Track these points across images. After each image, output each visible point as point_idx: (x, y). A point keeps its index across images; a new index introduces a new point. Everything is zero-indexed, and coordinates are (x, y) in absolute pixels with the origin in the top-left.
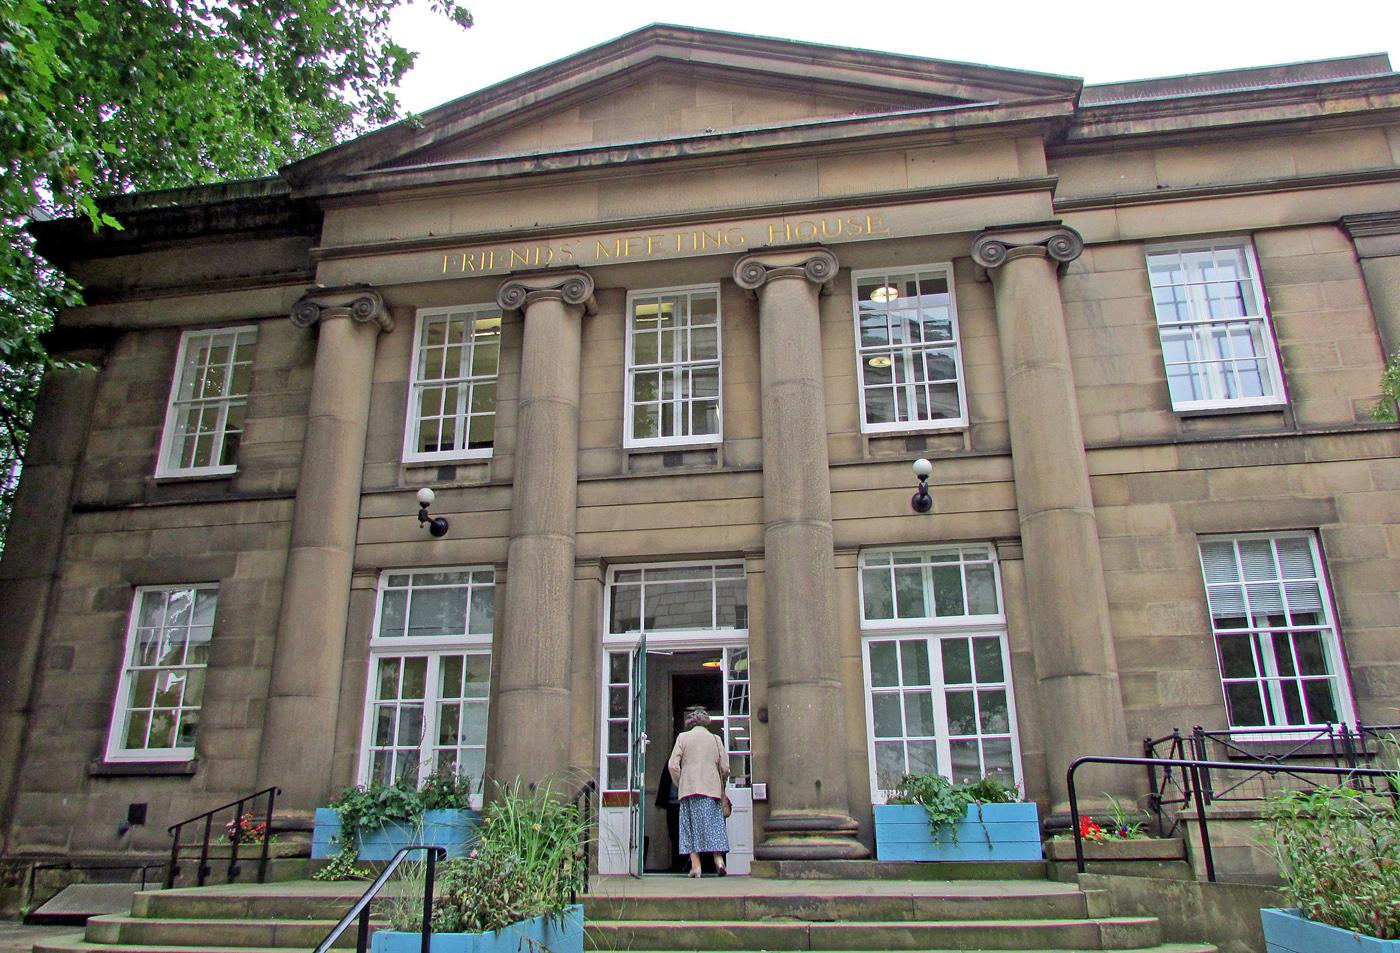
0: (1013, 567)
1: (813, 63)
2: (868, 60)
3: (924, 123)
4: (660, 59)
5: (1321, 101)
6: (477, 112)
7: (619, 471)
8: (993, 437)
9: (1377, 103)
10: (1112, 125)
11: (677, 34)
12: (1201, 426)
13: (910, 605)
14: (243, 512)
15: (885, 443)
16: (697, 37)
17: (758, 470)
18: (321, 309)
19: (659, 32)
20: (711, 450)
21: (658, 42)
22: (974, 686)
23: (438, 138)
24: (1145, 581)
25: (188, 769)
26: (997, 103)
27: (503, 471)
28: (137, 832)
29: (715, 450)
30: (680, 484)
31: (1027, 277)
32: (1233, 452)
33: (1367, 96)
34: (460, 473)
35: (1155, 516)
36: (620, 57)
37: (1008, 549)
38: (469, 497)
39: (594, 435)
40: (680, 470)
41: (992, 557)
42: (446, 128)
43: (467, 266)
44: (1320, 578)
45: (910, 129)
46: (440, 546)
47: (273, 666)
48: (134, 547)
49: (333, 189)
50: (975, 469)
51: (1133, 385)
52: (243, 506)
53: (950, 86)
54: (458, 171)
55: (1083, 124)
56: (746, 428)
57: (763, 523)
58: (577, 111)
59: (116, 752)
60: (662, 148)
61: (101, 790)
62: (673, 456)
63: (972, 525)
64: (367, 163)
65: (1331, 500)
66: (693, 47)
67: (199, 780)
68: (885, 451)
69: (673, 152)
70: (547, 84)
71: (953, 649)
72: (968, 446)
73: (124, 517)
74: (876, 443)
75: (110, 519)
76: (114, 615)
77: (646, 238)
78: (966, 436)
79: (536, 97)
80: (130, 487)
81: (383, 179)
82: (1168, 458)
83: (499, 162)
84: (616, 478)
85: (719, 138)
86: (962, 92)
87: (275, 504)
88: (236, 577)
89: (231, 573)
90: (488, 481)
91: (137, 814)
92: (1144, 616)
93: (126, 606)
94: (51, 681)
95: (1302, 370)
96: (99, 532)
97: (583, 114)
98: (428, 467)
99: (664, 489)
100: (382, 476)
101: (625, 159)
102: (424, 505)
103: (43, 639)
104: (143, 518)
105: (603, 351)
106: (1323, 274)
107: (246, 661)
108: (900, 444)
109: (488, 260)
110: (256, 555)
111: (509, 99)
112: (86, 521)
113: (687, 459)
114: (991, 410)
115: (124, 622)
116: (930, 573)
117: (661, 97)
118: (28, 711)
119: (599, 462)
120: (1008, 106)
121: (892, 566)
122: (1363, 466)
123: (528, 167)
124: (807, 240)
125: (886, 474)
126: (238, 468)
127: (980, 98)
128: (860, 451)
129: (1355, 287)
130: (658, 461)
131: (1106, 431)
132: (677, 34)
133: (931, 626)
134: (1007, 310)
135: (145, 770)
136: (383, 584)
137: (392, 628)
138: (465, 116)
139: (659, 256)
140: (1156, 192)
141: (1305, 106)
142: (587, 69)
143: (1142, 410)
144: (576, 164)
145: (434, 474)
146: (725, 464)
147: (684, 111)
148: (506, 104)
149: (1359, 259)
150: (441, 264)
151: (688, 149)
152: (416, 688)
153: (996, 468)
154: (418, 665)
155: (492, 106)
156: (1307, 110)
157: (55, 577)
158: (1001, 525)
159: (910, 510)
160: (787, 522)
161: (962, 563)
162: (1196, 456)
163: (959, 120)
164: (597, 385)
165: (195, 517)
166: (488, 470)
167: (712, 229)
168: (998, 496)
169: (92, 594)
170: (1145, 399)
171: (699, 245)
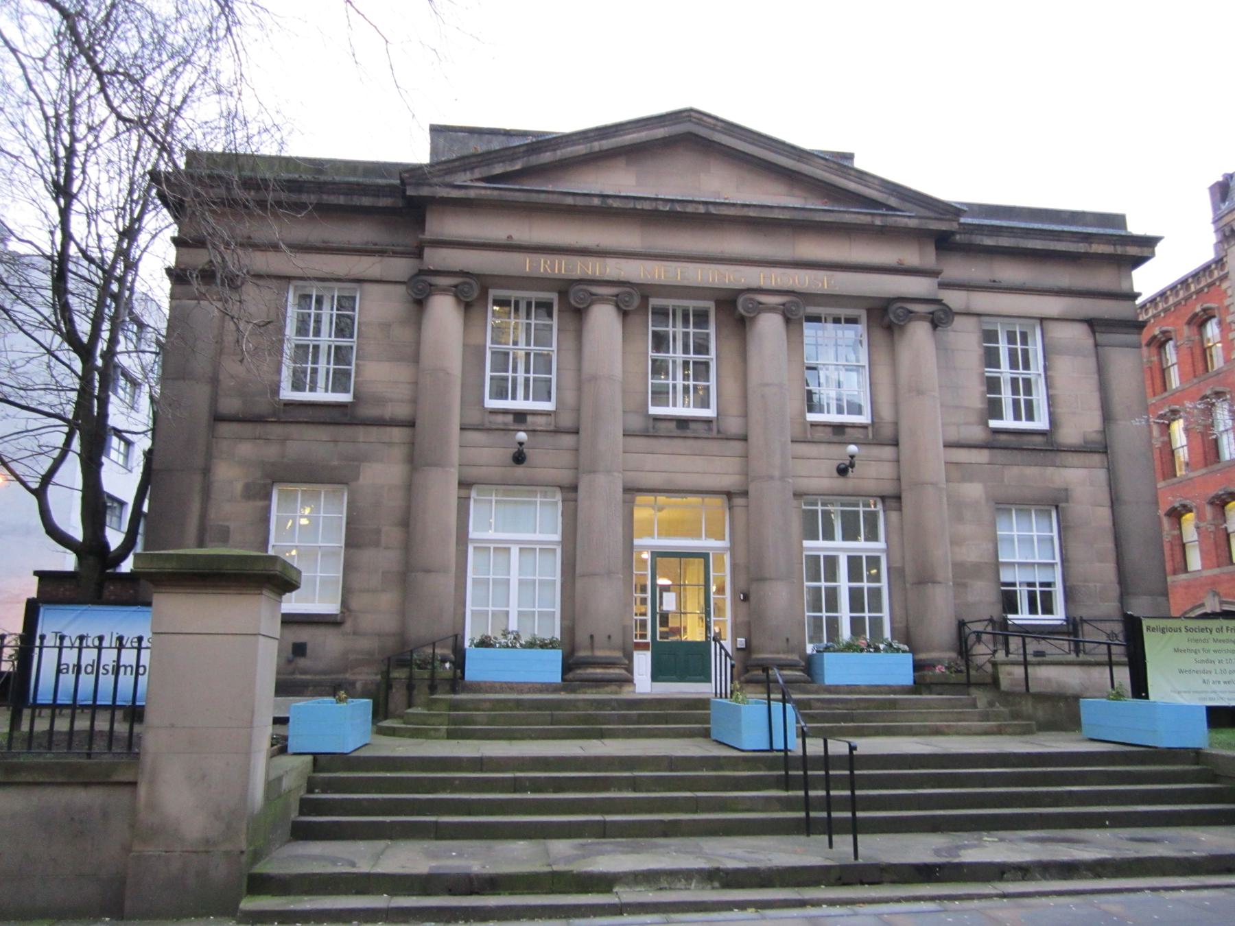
0: (894, 515)
1: (798, 161)
3: (868, 219)
4: (690, 134)
5: (1091, 243)
6: (555, 150)
7: (647, 430)
8: (887, 432)
9: (1119, 250)
10: (973, 237)
11: (705, 118)
12: (1003, 437)
13: (829, 535)
14: (361, 433)
15: (819, 428)
16: (720, 124)
17: (744, 439)
18: (431, 285)
19: (693, 114)
20: (708, 421)
21: (690, 121)
22: (823, 584)
24: (967, 529)
25: (339, 619)
26: (913, 214)
27: (566, 420)
28: (302, 662)
30: (690, 442)
31: (919, 333)
32: (1018, 456)
33: (1114, 245)
34: (529, 418)
35: (974, 491)
36: (663, 127)
37: (893, 503)
38: (541, 439)
40: (689, 433)
41: (880, 507)
43: (545, 269)
44: (1055, 534)
46: (520, 471)
47: (407, 546)
48: (271, 452)
50: (876, 451)
53: (885, 196)
54: (543, 196)
56: (734, 408)
57: (745, 473)
62: (683, 423)
63: (871, 486)
65: (1066, 490)
66: (717, 131)
67: (348, 626)
68: (820, 434)
69: (702, 209)
70: (607, 138)
71: (854, 562)
72: (870, 436)
73: (259, 429)
74: (813, 428)
75: (247, 429)
76: (261, 503)
77: (676, 268)
78: (870, 429)
79: (600, 145)
80: (262, 406)
81: (483, 192)
82: (982, 456)
83: (574, 194)
84: (645, 434)
85: (734, 205)
86: (893, 202)
87: (388, 429)
89: (356, 478)
90: (552, 428)
93: (268, 497)
95: (1061, 410)
96: (240, 439)
98: (505, 412)
100: (474, 417)
101: (667, 209)
102: (521, 444)
103: (203, 516)
104: (277, 430)
107: (376, 544)
109: (561, 267)
111: (579, 144)
112: (225, 429)
113: (692, 425)
114: (886, 414)
115: (268, 509)
116: (839, 513)
119: (636, 423)
120: (920, 218)
121: (820, 508)
123: (596, 202)
124: (786, 287)
125: (823, 449)
127: (903, 209)
128: (805, 432)
129: (1091, 363)
131: (953, 436)
132: (705, 118)
133: (841, 548)
134: (905, 356)
138: (546, 151)
139: (685, 283)
141: (1081, 245)
142: (639, 132)
145: (510, 418)
146: (719, 432)
149: (1096, 345)
150: (526, 264)
151: (713, 210)
153: (888, 452)
156: (1081, 247)
157: (206, 471)
158: (888, 488)
159: (835, 474)
160: (771, 478)
161: (861, 509)
162: (1000, 455)
163: (891, 221)
165: (322, 433)
167: (723, 268)
168: (887, 470)
169: (239, 487)
171: (714, 280)
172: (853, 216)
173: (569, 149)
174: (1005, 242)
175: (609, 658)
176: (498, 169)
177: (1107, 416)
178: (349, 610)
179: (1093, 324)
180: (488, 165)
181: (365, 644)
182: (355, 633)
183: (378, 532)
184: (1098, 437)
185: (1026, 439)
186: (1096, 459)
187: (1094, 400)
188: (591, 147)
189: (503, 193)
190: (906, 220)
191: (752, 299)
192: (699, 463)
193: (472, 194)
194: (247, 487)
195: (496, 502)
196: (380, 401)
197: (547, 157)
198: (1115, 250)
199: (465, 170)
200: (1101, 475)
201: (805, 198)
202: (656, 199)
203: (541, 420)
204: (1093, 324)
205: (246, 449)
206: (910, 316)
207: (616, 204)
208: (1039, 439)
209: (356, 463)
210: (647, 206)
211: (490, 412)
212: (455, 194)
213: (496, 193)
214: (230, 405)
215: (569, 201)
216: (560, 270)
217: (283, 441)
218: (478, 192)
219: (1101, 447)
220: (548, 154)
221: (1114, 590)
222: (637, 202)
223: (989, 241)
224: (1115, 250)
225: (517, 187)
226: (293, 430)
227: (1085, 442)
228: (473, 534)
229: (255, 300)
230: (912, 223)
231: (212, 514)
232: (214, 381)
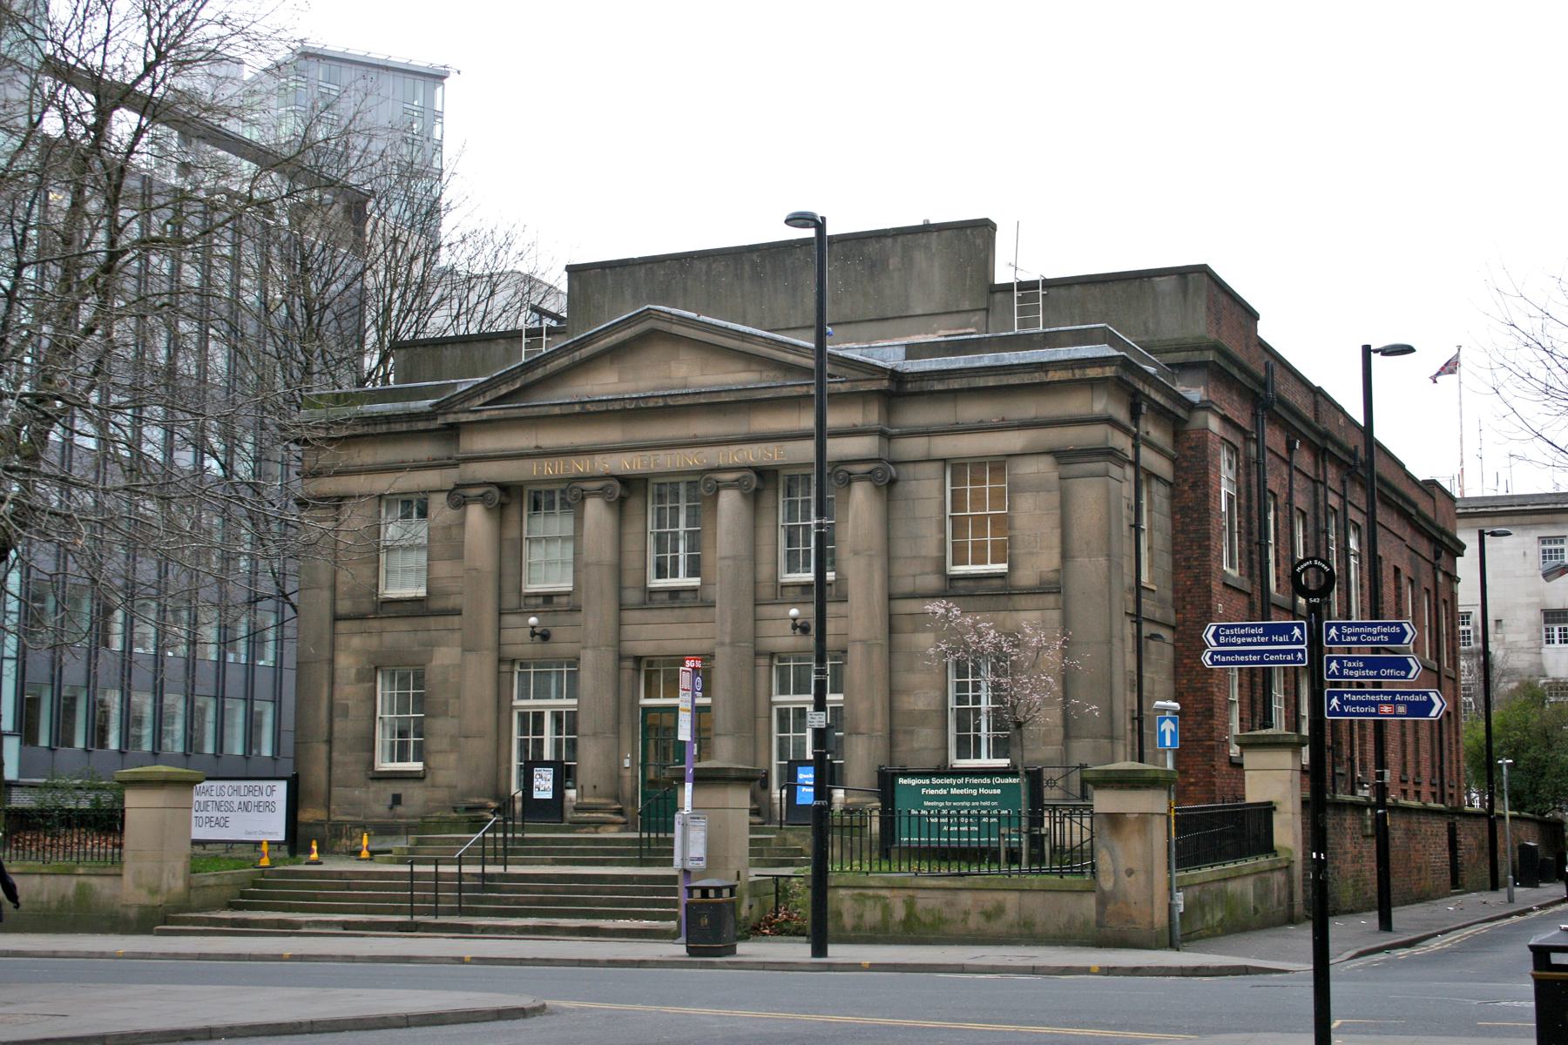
5: (1047, 371)
9: (1078, 374)
11: (662, 314)
14: (432, 622)
15: (791, 589)
25: (421, 775)
28: (399, 809)
29: (696, 590)
30: (677, 612)
34: (555, 600)
36: (629, 328)
38: (562, 618)
39: (629, 580)
45: (795, 394)
48: (373, 642)
49: (464, 418)
51: (925, 557)
52: (432, 619)
54: (536, 409)
55: (908, 382)
58: (609, 356)
59: (384, 765)
60: (655, 400)
61: (376, 786)
62: (674, 593)
64: (482, 401)
67: (428, 780)
68: (790, 593)
69: (661, 403)
70: (585, 347)
76: (371, 684)
78: (834, 586)
81: (493, 412)
88: (434, 663)
89: (431, 661)
91: (397, 799)
92: (912, 700)
93: (376, 682)
94: (338, 725)
96: (353, 634)
97: (612, 361)
99: (666, 615)
101: (633, 406)
104: (375, 624)
105: (633, 529)
106: (1038, 488)
107: (445, 714)
108: (798, 589)
110: (444, 649)
112: (342, 626)
113: (683, 595)
117: (658, 351)
118: (330, 742)
120: (851, 381)
122: (1038, 614)
123: (577, 408)
126: (427, 593)
129: (1055, 498)
130: (665, 596)
132: (662, 314)
135: (393, 775)
136: (517, 668)
137: (524, 695)
138: (537, 368)
141: (1036, 374)
143: (928, 574)
144: (604, 408)
145: (540, 600)
146: (702, 600)
147: (673, 363)
148: (562, 360)
151: (670, 402)
152: (539, 730)
154: (539, 717)
156: (1037, 377)
157: (332, 661)
164: (632, 545)
166: (571, 598)
169: (353, 672)
170: (929, 567)
172: (790, 389)
173: (556, 362)
175: (592, 804)
176: (504, 390)
177: (1065, 555)
178: (430, 768)
179: (1062, 456)
180: (495, 388)
181: (441, 794)
182: (433, 786)
183: (446, 703)
184: (1052, 576)
185: (985, 583)
186: (1050, 600)
187: (1055, 539)
189: (507, 411)
190: (839, 385)
191: (710, 479)
192: (683, 631)
193: (485, 415)
194: (359, 672)
196: (447, 594)
197: (539, 373)
198: (1074, 375)
200: (1055, 615)
201: (761, 371)
203: (564, 600)
204: (1062, 456)
205: (356, 642)
206: (848, 481)
208: (996, 583)
209: (429, 648)
210: (617, 406)
212: (472, 417)
213: (502, 412)
214: (344, 606)
215: (557, 410)
216: (559, 471)
217: (381, 633)
218: (488, 413)
219: (1052, 588)
220: (540, 370)
221: (1058, 735)
222: (609, 404)
223: (939, 386)
224: (1074, 375)
226: (386, 624)
227: (1041, 583)
229: (355, 519)
230: (843, 388)
231: (337, 695)
232: (334, 588)
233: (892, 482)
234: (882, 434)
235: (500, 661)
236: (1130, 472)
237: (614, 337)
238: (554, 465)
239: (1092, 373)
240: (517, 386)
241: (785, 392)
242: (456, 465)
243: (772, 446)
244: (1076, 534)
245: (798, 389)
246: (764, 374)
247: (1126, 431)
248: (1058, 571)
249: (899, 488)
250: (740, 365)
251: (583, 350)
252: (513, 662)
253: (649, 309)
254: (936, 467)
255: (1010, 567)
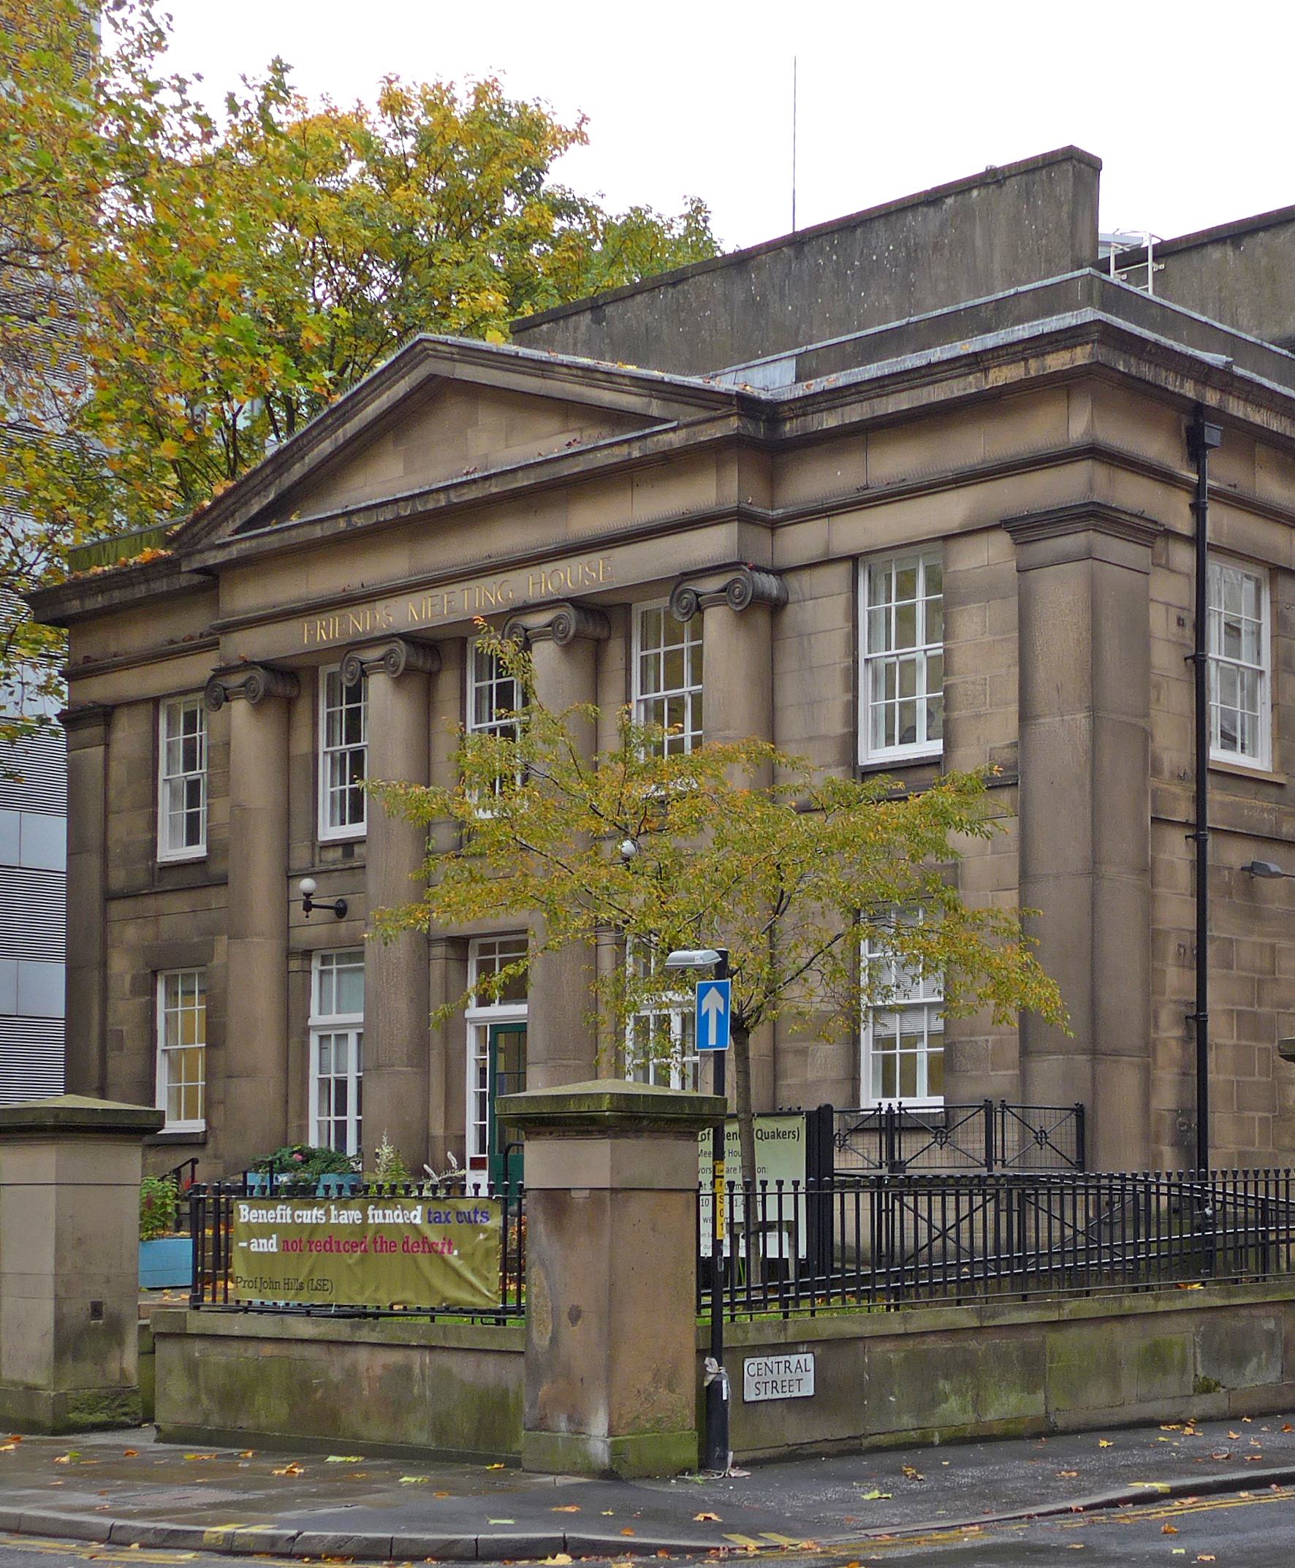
2: (580, 373)
3: (620, 454)
4: (432, 378)
5: (986, 370)
6: (303, 458)
9: (1034, 367)
21: (429, 356)
23: (279, 492)
25: (200, 1140)
36: (403, 377)
42: (283, 479)
55: (785, 420)
64: (231, 526)
70: (350, 419)
86: (655, 409)
89: (211, 959)
93: (154, 993)
102: (308, 895)
104: (151, 904)
106: (989, 593)
111: (324, 440)
112: (117, 908)
120: (687, 426)
123: (342, 524)
126: (208, 851)
127: (669, 417)
132: (440, 347)
136: (316, 965)
138: (295, 464)
140: (858, 496)
155: (313, 450)
157: (104, 964)
163: (652, 445)
169: (128, 978)
170: (831, 754)
172: (606, 452)
173: (316, 450)
174: (855, 413)
178: (210, 1128)
188: (336, 439)
189: (261, 540)
190: (671, 435)
193: (234, 552)
195: (340, 971)
199: (226, 519)
202: (396, 501)
205: (131, 933)
207: (359, 521)
210: (387, 515)
211: (321, 847)
214: (118, 879)
217: (158, 915)
220: (298, 465)
223: (830, 421)
225: (267, 529)
228: (315, 1018)
230: (676, 439)
231: (110, 1020)
233: (775, 607)
234: (742, 516)
235: (289, 954)
236: (1184, 557)
237: (384, 397)
238: (328, 625)
239: (1057, 362)
240: (272, 497)
241: (602, 459)
242: (215, 645)
243: (596, 558)
244: (1042, 673)
245: (616, 450)
246: (587, 433)
247: (1165, 477)
248: (1015, 745)
249: (792, 614)
250: (551, 424)
251: (347, 426)
252: (307, 954)
253: (421, 340)
254: (842, 570)
255: (946, 747)
